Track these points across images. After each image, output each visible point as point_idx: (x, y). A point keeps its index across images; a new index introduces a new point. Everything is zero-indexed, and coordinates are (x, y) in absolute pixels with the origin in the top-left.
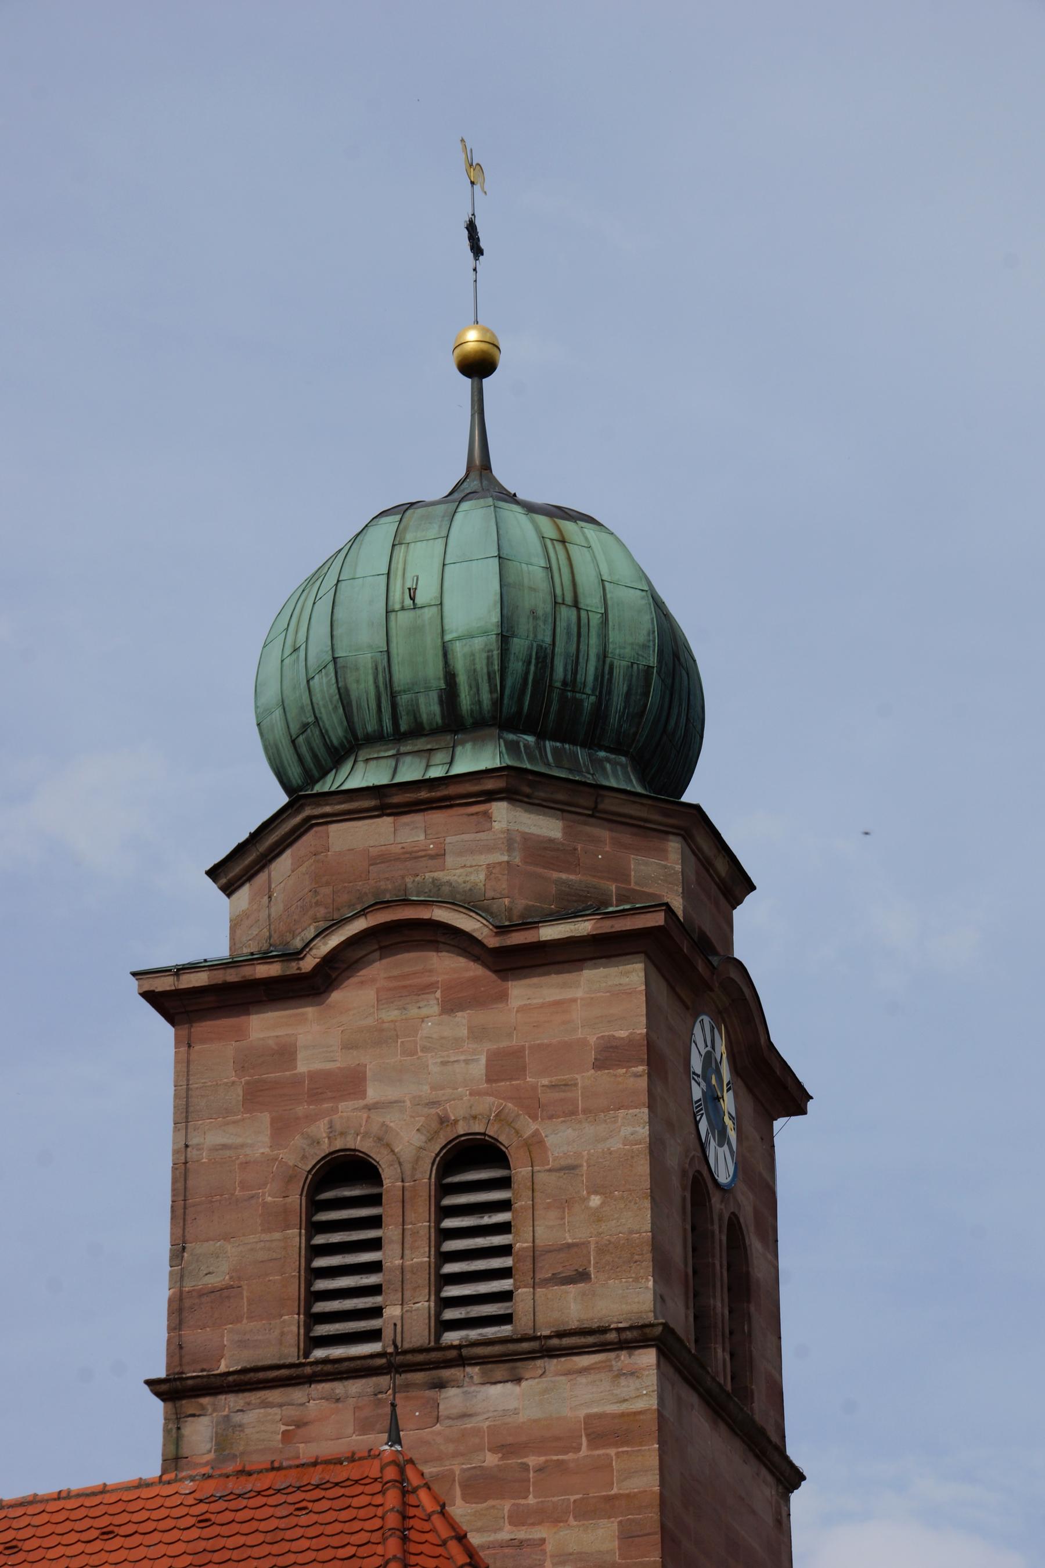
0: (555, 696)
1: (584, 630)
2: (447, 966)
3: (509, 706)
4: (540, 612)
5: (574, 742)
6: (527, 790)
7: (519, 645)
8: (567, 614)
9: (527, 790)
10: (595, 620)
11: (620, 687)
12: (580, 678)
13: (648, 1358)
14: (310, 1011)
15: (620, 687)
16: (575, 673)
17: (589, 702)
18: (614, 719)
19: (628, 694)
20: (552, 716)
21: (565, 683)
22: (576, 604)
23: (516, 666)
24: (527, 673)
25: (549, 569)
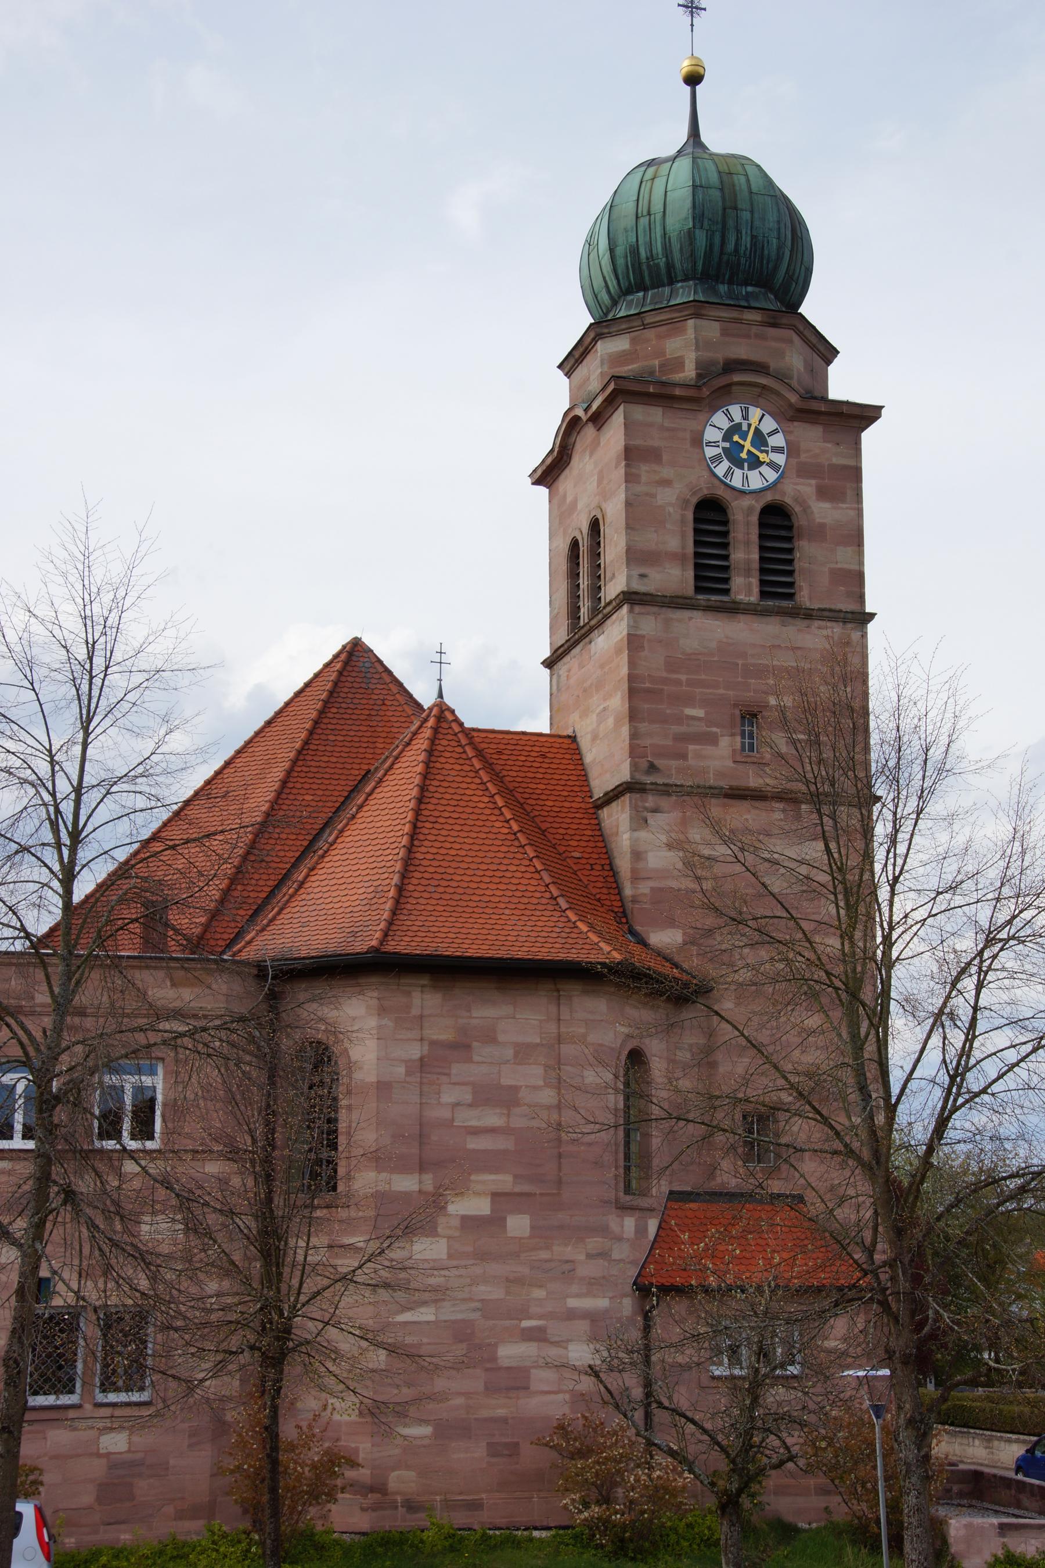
0: (644, 267)
1: (652, 226)
2: (590, 431)
3: (624, 284)
4: (629, 227)
5: (663, 286)
6: (606, 331)
7: (620, 251)
8: (644, 221)
9: (606, 331)
10: (659, 217)
11: (676, 247)
12: (654, 252)
13: (625, 609)
14: (567, 472)
15: (676, 247)
16: (651, 251)
17: (662, 262)
18: (678, 265)
19: (681, 249)
20: (647, 278)
21: (647, 259)
22: (649, 214)
23: (620, 262)
24: (627, 262)
25: (638, 200)
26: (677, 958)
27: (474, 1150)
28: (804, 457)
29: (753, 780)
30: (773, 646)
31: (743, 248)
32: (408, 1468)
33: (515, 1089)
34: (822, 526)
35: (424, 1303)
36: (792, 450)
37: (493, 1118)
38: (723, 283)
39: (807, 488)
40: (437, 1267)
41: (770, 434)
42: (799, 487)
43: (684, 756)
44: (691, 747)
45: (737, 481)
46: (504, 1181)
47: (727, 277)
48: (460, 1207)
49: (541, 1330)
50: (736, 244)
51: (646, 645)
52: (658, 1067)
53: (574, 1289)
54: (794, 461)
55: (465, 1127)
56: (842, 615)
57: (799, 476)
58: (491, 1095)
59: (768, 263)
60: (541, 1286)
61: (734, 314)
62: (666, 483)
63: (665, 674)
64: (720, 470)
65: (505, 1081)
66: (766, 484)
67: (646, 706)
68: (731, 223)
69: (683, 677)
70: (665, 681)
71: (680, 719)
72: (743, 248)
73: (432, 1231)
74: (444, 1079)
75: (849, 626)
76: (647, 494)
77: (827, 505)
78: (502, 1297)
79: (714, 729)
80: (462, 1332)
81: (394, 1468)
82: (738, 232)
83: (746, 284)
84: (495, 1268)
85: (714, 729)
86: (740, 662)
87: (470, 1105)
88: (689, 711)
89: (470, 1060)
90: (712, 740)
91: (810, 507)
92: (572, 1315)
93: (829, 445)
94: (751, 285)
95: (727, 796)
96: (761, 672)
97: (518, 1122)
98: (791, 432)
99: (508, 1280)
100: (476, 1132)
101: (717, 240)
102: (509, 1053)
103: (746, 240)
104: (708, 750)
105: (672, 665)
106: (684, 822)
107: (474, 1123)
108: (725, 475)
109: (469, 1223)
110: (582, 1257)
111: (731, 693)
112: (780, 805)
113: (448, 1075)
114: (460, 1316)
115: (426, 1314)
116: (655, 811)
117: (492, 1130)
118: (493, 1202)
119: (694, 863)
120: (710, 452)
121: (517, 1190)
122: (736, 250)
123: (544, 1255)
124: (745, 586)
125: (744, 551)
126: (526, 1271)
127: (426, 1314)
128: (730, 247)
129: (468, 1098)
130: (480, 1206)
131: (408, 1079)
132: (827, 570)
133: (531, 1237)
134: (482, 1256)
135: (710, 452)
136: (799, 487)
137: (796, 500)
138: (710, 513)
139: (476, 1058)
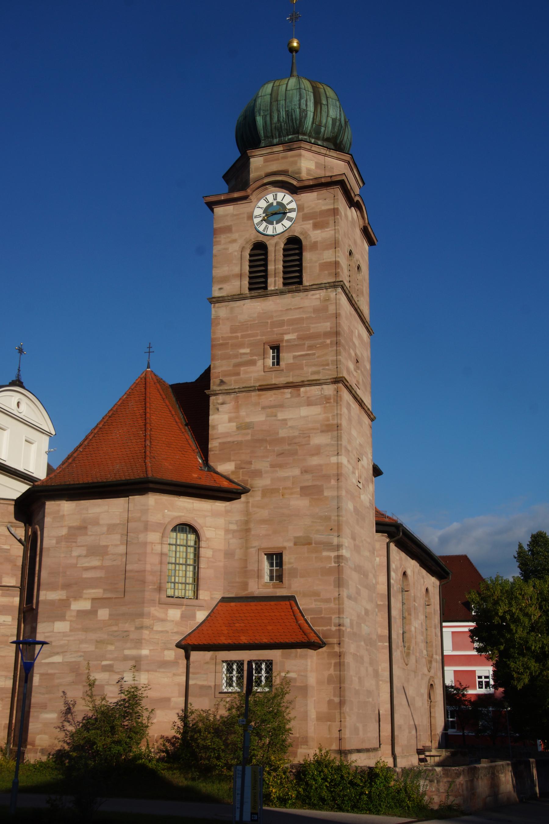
26: (232, 477)
27: (86, 578)
28: (306, 211)
29: (275, 380)
30: (287, 310)
31: (282, 118)
32: (45, 733)
33: (107, 547)
34: (316, 243)
35: (58, 653)
36: (300, 208)
37: (95, 562)
38: (276, 138)
39: (308, 225)
40: (65, 634)
41: (268, 202)
42: (303, 226)
43: (238, 374)
44: (242, 369)
45: (270, 232)
46: (98, 592)
47: (277, 135)
48: (77, 606)
49: (111, 666)
50: (278, 118)
51: (221, 322)
52: (207, 533)
53: (128, 645)
54: (301, 214)
55: (82, 567)
56: (323, 285)
57: (303, 221)
58: (96, 551)
59: (296, 122)
60: (112, 644)
61: (268, 150)
62: (234, 241)
63: (230, 335)
64: (261, 229)
65: (103, 543)
66: (285, 229)
67: (220, 352)
68: (274, 108)
69: (239, 335)
70: (231, 338)
71: (236, 356)
72: (282, 118)
73: (62, 618)
74: (74, 544)
75: (329, 290)
76: (224, 249)
77: (318, 232)
78: (93, 649)
79: (254, 358)
80: (74, 668)
81: (39, 734)
82: (278, 111)
83: (288, 135)
84: (93, 636)
85: (254, 358)
86: (269, 321)
87: (85, 556)
88: (242, 351)
89: (86, 534)
90: (253, 363)
91: (309, 235)
92: (126, 658)
93: (320, 201)
94: (291, 135)
95: (259, 390)
96: (282, 323)
97: (107, 563)
98: (300, 200)
99: (97, 641)
100: (87, 569)
101: (268, 118)
102: (105, 529)
103: (283, 114)
104: (252, 368)
105: (233, 330)
106: (237, 408)
107: (87, 565)
108: (264, 231)
109: (81, 613)
110: (133, 629)
111: (264, 337)
112: (289, 390)
113: (75, 542)
114: (73, 660)
115: (57, 659)
116: (223, 404)
117: (94, 568)
118: (92, 603)
119: (243, 427)
120: (256, 221)
121: (104, 596)
122: (278, 120)
123: (115, 628)
124: (275, 282)
125: (276, 264)
126: (106, 637)
127: (57, 659)
128: (275, 120)
129: (84, 553)
130: (86, 605)
131: (57, 546)
132: (317, 264)
133: (110, 619)
134: (86, 630)
135: (256, 221)
136: (303, 226)
137: (301, 233)
138: (259, 250)
139: (89, 533)
